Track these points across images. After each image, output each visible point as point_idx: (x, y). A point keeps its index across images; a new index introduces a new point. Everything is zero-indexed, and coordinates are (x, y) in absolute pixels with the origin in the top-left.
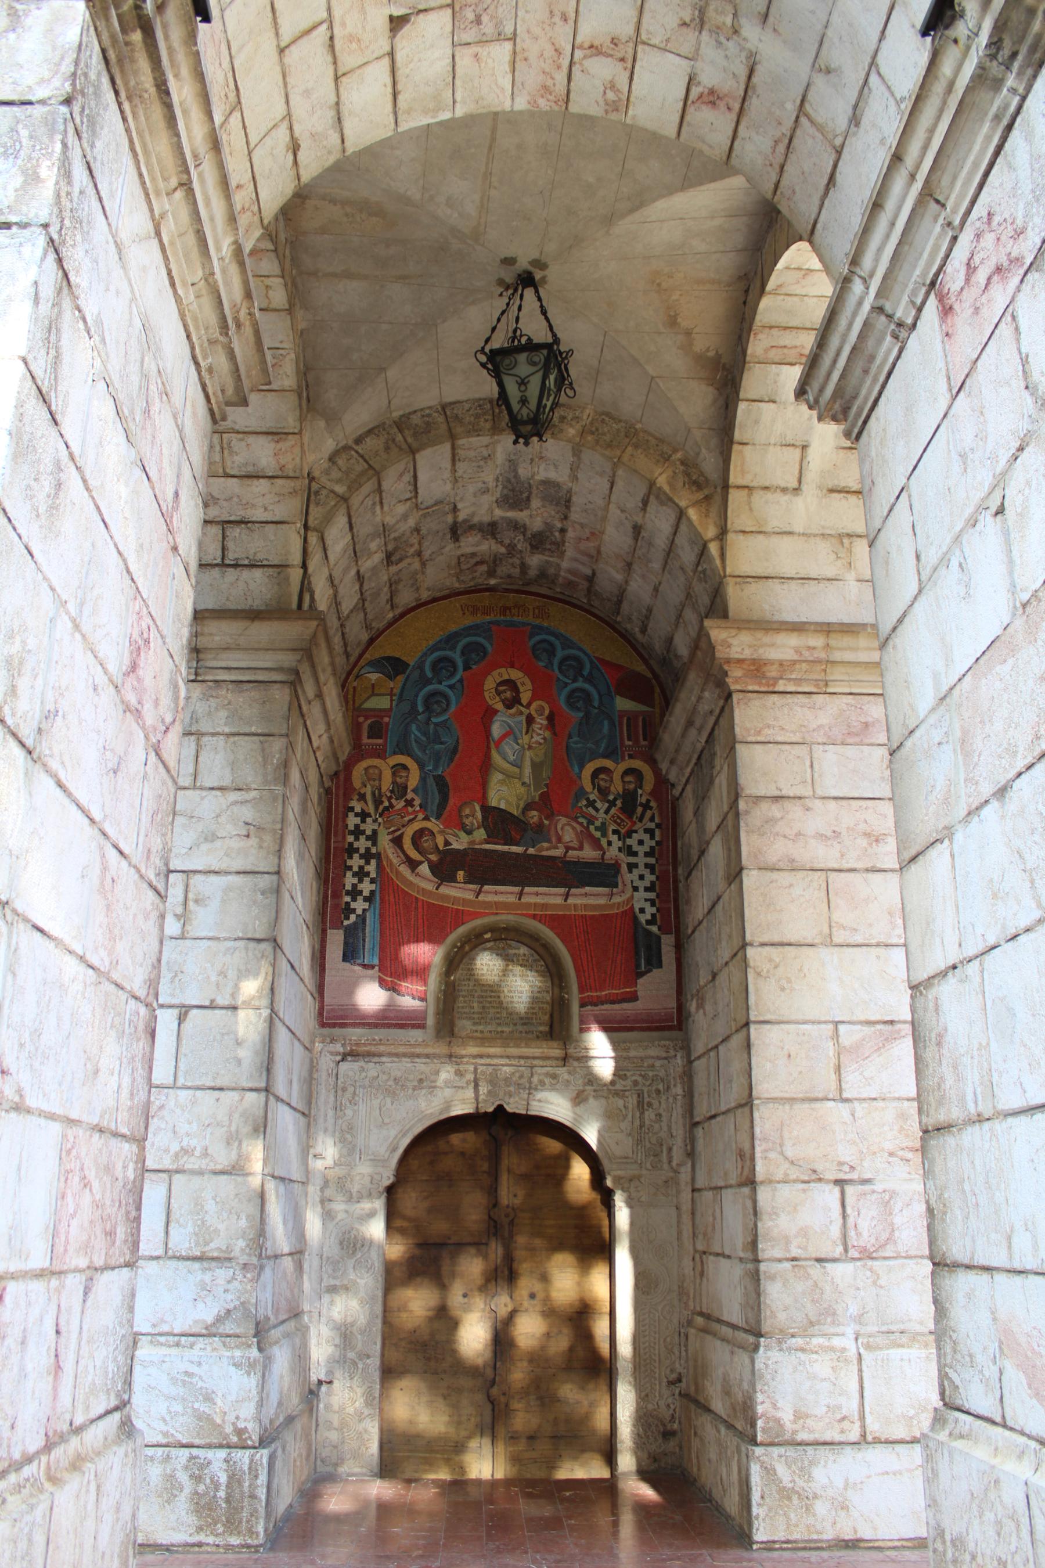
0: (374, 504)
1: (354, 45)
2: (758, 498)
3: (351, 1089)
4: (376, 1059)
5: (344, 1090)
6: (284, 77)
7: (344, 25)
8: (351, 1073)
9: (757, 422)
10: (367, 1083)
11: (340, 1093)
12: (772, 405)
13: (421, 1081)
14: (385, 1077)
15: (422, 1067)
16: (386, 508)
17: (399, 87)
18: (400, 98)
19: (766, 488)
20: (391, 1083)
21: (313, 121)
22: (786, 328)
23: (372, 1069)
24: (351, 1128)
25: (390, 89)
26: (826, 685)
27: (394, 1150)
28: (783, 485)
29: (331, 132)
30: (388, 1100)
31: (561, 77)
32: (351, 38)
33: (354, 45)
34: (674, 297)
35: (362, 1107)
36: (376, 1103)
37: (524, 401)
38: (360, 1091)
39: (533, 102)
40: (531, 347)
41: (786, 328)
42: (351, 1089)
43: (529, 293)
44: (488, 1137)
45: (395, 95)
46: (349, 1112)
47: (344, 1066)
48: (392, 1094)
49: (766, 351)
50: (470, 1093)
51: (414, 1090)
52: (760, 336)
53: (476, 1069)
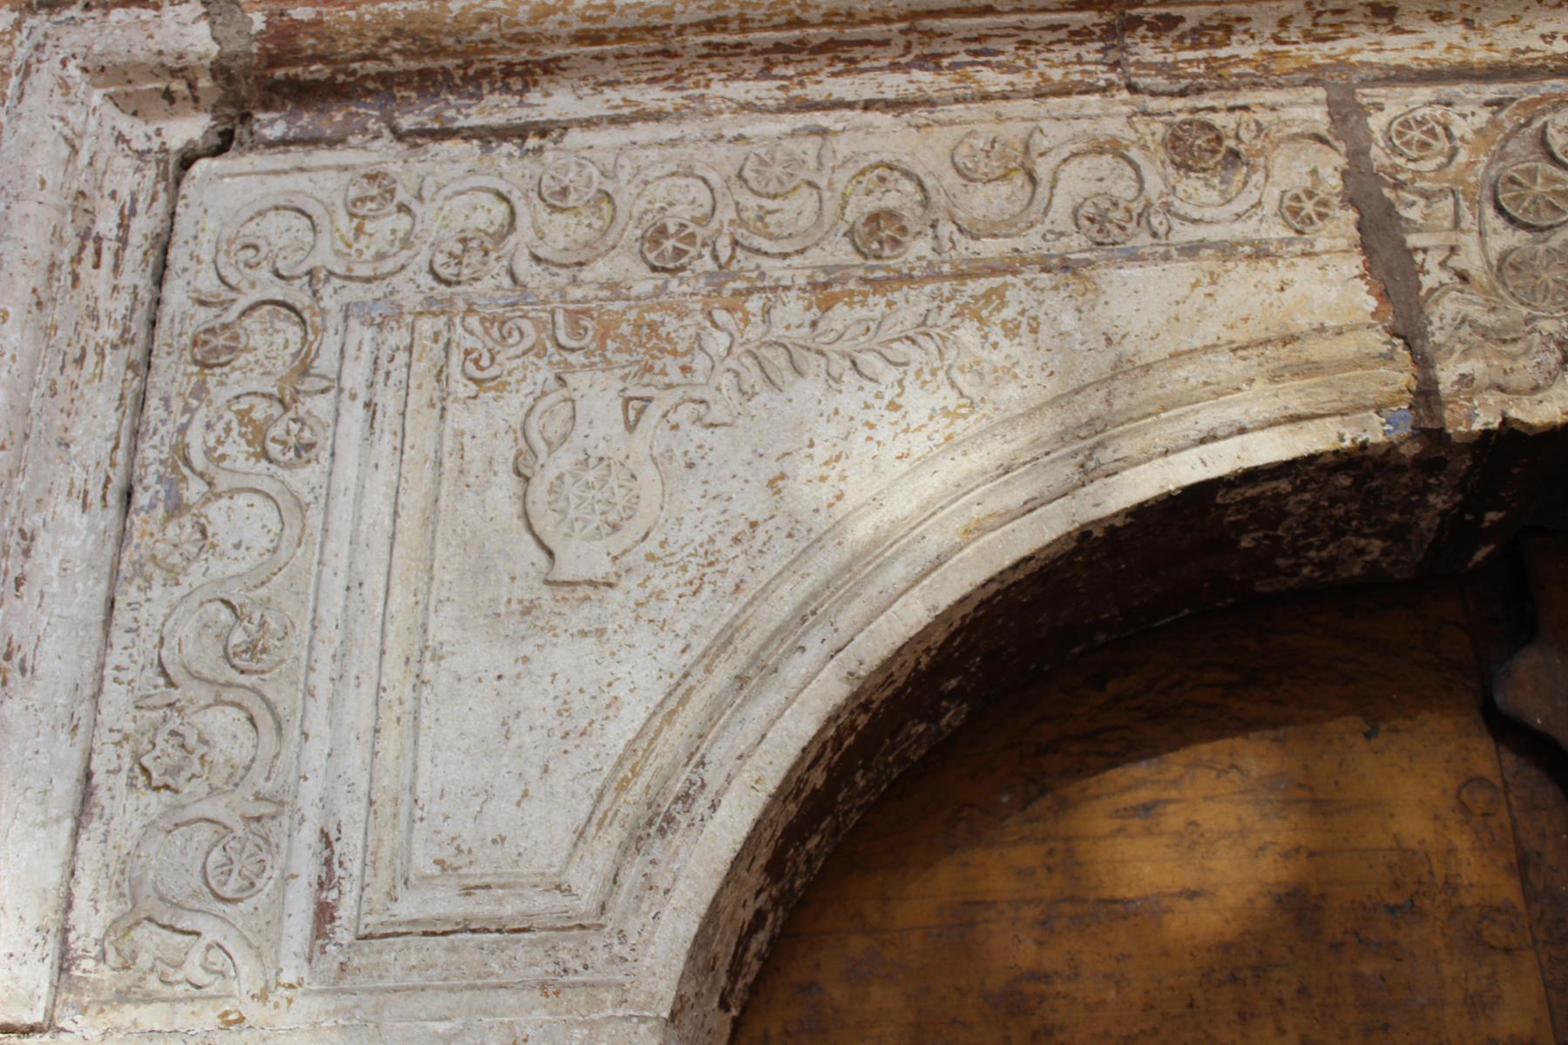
3: (273, 343)
4: (496, 109)
5: (211, 353)
8: (279, 231)
10: (412, 289)
11: (172, 373)
13: (881, 230)
14: (562, 233)
15: (888, 136)
20: (623, 265)
23: (455, 186)
24: (249, 650)
27: (658, 822)
30: (599, 396)
35: (362, 477)
36: (486, 425)
38: (349, 353)
42: (273, 343)
44: (1484, 757)
46: (243, 523)
47: (227, 190)
48: (639, 347)
50: (1330, 288)
51: (823, 291)
53: (1346, 115)
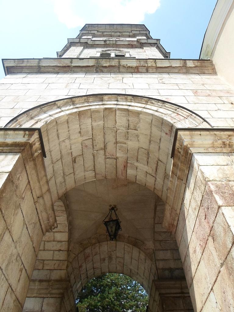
0: (165, 242)
1: (50, 238)
2: (157, 188)
6: (48, 250)
7: (46, 239)
9: (141, 180)
12: (137, 176)
16: (170, 239)
17: (60, 231)
18: (62, 231)
19: (155, 184)
21: (58, 246)
22: (116, 173)
25: (60, 233)
26: (177, 214)
28: (154, 181)
29: (62, 243)
31: (59, 211)
32: (49, 238)
33: (50, 238)
34: (119, 185)
37: (112, 231)
39: (65, 214)
40: (113, 221)
41: (116, 173)
43: (113, 211)
45: (61, 232)
49: (123, 176)
52: (119, 177)
